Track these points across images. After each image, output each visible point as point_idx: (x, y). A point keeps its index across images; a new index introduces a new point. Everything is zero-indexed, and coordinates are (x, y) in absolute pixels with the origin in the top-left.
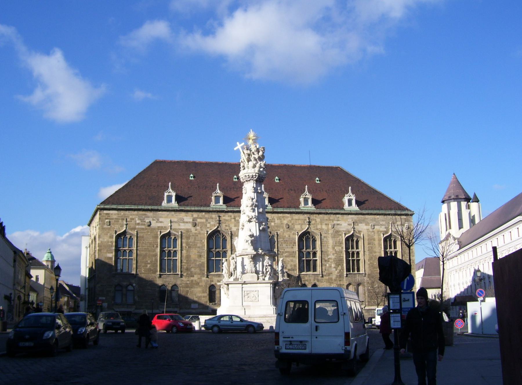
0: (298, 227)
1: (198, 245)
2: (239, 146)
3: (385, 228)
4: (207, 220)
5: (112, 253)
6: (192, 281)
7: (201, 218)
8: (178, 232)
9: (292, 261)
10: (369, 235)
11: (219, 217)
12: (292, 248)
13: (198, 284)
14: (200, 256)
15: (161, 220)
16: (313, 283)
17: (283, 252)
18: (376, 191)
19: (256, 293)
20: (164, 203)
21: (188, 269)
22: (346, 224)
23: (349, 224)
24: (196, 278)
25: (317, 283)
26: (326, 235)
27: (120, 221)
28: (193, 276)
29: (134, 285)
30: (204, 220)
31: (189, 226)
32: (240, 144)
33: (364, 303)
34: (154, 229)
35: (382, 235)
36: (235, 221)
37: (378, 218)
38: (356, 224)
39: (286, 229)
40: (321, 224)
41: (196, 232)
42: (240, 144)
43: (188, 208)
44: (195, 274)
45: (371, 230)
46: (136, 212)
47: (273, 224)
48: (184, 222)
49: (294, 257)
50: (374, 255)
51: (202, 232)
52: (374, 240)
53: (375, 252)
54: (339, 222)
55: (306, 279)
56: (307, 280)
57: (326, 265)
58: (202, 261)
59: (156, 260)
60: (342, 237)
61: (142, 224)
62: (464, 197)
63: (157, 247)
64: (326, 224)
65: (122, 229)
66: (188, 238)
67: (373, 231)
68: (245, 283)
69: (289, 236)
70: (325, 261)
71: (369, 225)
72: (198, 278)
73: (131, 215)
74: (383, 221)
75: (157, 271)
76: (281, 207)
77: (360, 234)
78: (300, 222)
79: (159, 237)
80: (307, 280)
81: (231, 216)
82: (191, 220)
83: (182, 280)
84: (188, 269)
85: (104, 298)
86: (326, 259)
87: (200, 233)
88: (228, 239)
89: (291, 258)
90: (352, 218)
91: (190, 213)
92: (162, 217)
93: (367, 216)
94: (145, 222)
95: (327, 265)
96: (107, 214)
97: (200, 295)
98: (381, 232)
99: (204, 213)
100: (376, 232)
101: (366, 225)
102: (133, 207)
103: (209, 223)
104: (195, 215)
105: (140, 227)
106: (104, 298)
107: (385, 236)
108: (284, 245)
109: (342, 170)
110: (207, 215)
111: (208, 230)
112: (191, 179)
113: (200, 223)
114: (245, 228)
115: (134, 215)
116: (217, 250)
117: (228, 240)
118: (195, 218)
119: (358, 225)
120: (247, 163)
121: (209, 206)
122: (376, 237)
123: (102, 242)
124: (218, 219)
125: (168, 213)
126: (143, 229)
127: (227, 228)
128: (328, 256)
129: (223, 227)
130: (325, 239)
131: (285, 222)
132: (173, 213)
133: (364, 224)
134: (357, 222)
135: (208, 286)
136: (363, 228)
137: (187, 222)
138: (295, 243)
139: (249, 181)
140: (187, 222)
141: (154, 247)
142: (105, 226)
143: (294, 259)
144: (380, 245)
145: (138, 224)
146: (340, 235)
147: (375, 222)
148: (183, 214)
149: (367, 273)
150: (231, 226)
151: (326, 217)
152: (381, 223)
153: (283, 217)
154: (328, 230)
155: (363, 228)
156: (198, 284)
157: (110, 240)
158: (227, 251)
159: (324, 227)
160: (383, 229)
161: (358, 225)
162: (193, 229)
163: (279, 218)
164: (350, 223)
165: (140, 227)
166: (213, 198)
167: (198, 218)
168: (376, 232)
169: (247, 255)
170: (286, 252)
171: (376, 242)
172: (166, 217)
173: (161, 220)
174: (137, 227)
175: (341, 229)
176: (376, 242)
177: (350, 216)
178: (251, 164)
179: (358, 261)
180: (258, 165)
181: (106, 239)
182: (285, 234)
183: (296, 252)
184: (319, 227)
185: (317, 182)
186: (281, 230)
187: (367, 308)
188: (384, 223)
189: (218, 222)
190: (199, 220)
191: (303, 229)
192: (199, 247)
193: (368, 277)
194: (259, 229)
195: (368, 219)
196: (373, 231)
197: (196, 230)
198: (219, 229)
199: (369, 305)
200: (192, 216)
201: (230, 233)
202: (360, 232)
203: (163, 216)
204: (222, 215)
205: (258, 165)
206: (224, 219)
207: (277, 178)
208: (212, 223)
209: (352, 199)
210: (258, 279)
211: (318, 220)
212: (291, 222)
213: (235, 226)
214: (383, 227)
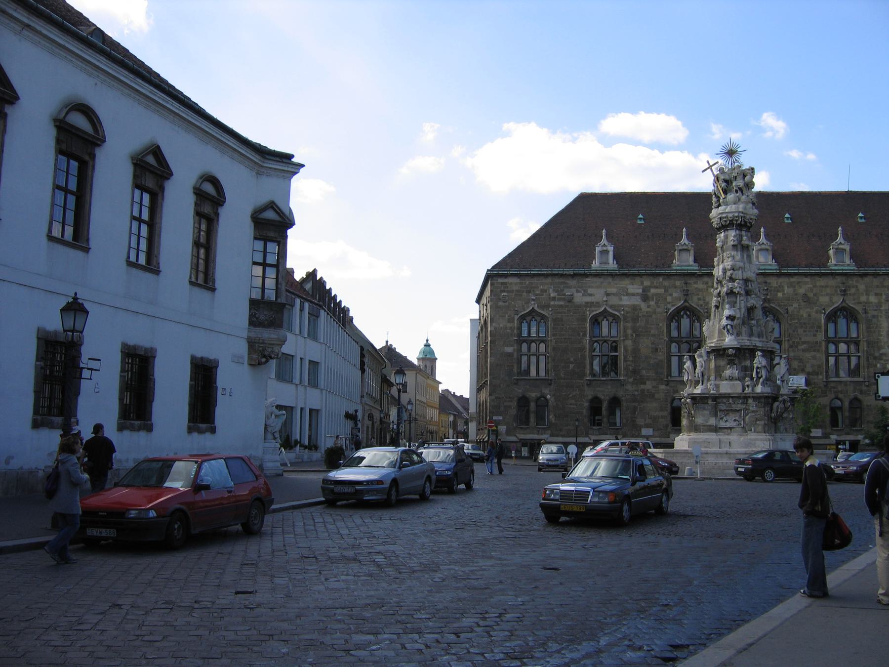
0: (824, 300)
1: (652, 332)
4: (666, 291)
5: (512, 346)
6: (643, 391)
7: (656, 287)
8: (619, 311)
9: (814, 358)
12: (815, 335)
13: (652, 396)
14: (656, 350)
15: (590, 291)
16: (852, 396)
17: (798, 343)
20: (596, 264)
21: (635, 372)
24: (648, 386)
25: (860, 396)
26: (875, 313)
27: (525, 294)
28: (645, 384)
29: (548, 397)
30: (661, 291)
31: (637, 301)
34: (579, 306)
39: (803, 304)
40: (868, 295)
41: (649, 310)
43: (634, 271)
44: (648, 379)
46: (549, 280)
47: (780, 295)
48: (628, 294)
49: (818, 351)
51: (659, 310)
55: (840, 389)
56: (841, 392)
57: (876, 366)
58: (659, 358)
59: (584, 357)
61: (559, 300)
63: (585, 335)
64: (876, 294)
65: (528, 307)
66: (635, 320)
69: (809, 315)
70: (875, 358)
72: (653, 387)
75: (585, 375)
76: (794, 266)
78: (828, 291)
80: (841, 392)
81: (707, 283)
82: (640, 291)
83: (627, 390)
84: (635, 372)
85: (501, 418)
86: (877, 354)
87: (655, 312)
89: (813, 353)
91: (638, 279)
92: (592, 287)
94: (564, 295)
95: (878, 365)
96: (502, 284)
97: (657, 413)
99: (661, 279)
102: (545, 271)
103: (671, 295)
104: (647, 283)
106: (501, 418)
108: (800, 331)
110: (666, 283)
111: (669, 306)
112: (639, 222)
113: (657, 294)
118: (646, 287)
121: (669, 267)
123: (495, 328)
125: (601, 280)
126: (561, 306)
127: (701, 302)
128: (879, 348)
129: (694, 302)
130: (874, 320)
131: (802, 291)
132: (610, 279)
135: (669, 399)
137: (633, 295)
138: (820, 327)
140: (633, 295)
141: (579, 335)
142: (501, 303)
143: (818, 355)
145: (554, 299)
148: (626, 283)
151: (876, 281)
153: (799, 283)
154: (879, 305)
156: (652, 396)
157: (509, 325)
159: (873, 299)
162: (643, 306)
163: (791, 285)
167: (651, 287)
170: (804, 343)
172: (598, 287)
173: (590, 291)
174: (552, 303)
181: (503, 323)
182: (802, 312)
183: (821, 343)
184: (863, 298)
185: (860, 221)
186: (796, 305)
190: (653, 291)
191: (833, 304)
192: (654, 335)
197: (649, 307)
200: (642, 283)
204: (691, 281)
207: (787, 215)
208: (675, 295)
210: (744, 390)
211: (862, 287)
212: (812, 291)
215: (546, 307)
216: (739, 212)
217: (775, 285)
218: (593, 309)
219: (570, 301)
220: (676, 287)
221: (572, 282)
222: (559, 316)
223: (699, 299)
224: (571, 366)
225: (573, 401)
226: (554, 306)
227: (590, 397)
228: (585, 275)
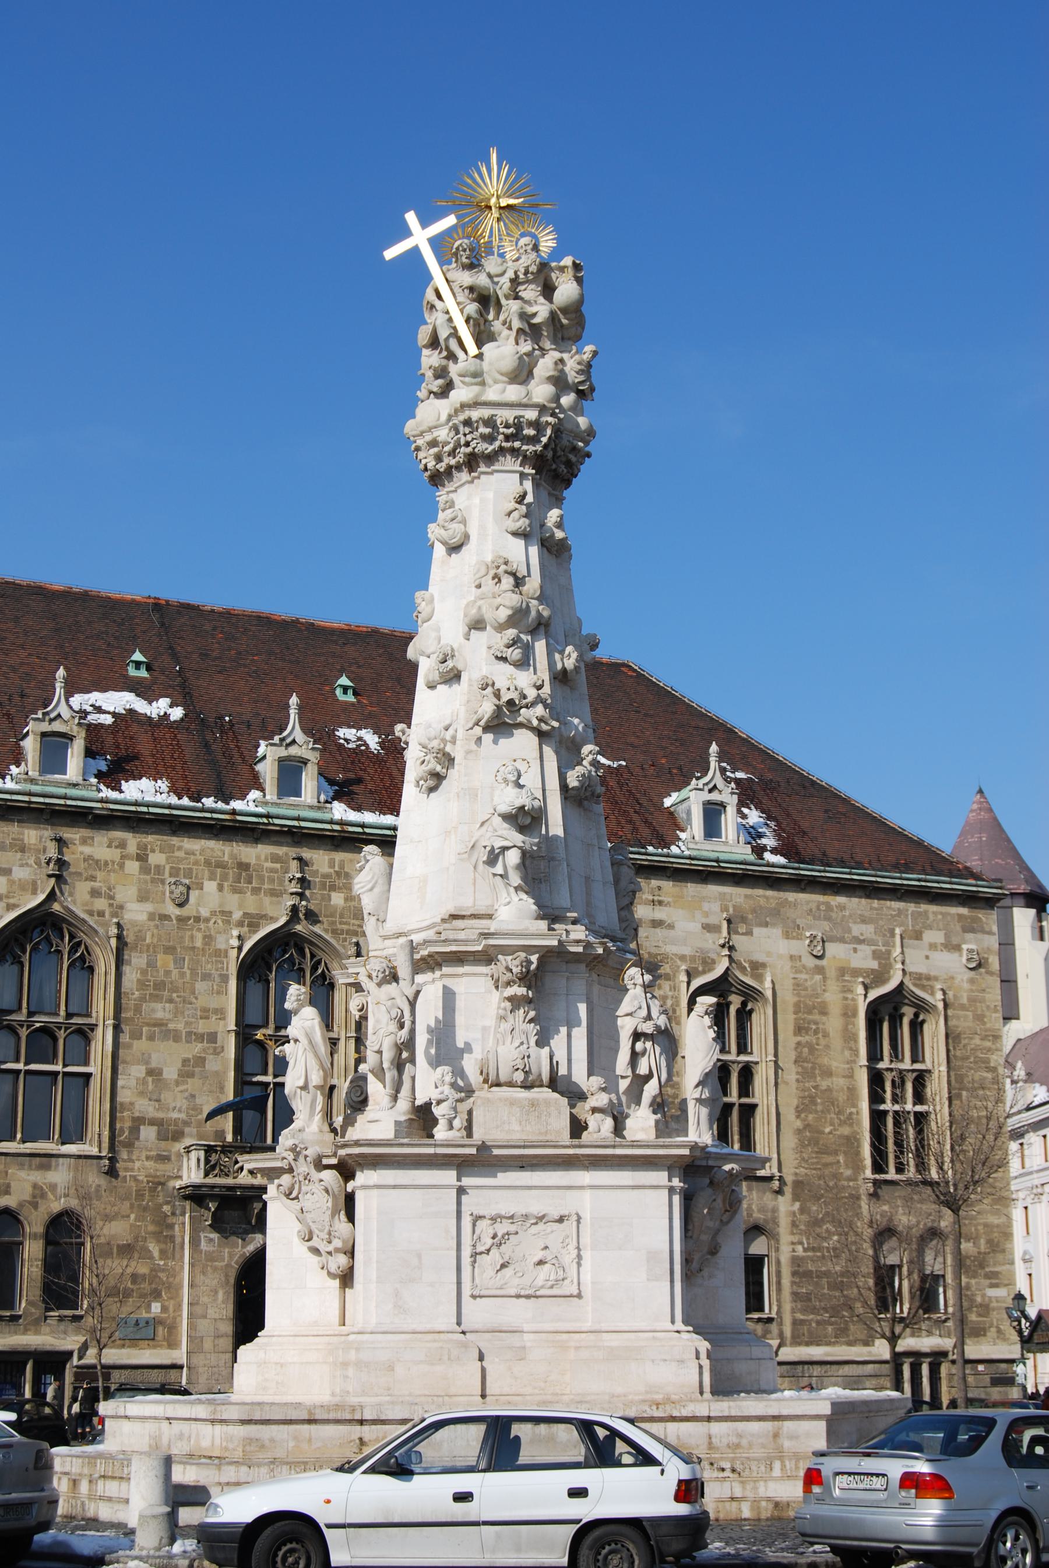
2: (420, 236)
3: (876, 955)
10: (798, 986)
11: (60, 842)
18: (813, 783)
19: (555, 1234)
22: (695, 927)
23: (708, 928)
32: (425, 223)
33: (774, 1327)
35: (860, 990)
36: (145, 869)
37: (842, 908)
38: (742, 928)
42: (425, 223)
45: (811, 962)
50: (824, 1084)
52: (824, 1012)
53: (828, 1073)
54: (659, 914)
60: (674, 988)
62: (1023, 888)
67: (820, 970)
68: (481, 1161)
71: (800, 937)
74: (864, 921)
77: (760, 978)
81: (122, 845)
88: (104, 962)
90: (722, 896)
93: (792, 896)
98: (856, 972)
100: (832, 973)
101: (787, 936)
107: (873, 995)
109: (641, 679)
114: (454, 777)
116: (40, 1020)
117: (100, 968)
119: (749, 933)
120: (472, 349)
122: (832, 997)
124: (52, 852)
127: (101, 904)
129: (77, 900)
133: (776, 932)
134: (743, 919)
136: (774, 951)
139: (490, 458)
144: (850, 1037)
146: (667, 977)
147: (826, 925)
149: (789, 1179)
150: (119, 897)
152: (857, 929)
155: (774, 951)
158: (93, 1027)
160: (864, 959)
161: (749, 933)
164: (713, 920)
166: (30, 745)
168: (832, 973)
169: (487, 957)
171: (833, 1024)
175: (671, 949)
176: (833, 1024)
177: (713, 889)
178: (504, 351)
179: (748, 1111)
180: (545, 366)
187: (789, 1353)
188: (867, 930)
189: (52, 869)
193: (796, 1197)
194: (564, 787)
195: (795, 904)
196: (820, 970)
198: (56, 907)
199: (797, 1340)
201: (114, 931)
202: (757, 967)
205: (545, 366)
206: (88, 859)
207: (344, 681)
208: (20, 873)
209: (723, 806)
210: (577, 1128)
213: (143, 898)
214: (866, 950)
216: (542, 409)
217: (325, 869)
220: (23, 849)
223: (95, 893)
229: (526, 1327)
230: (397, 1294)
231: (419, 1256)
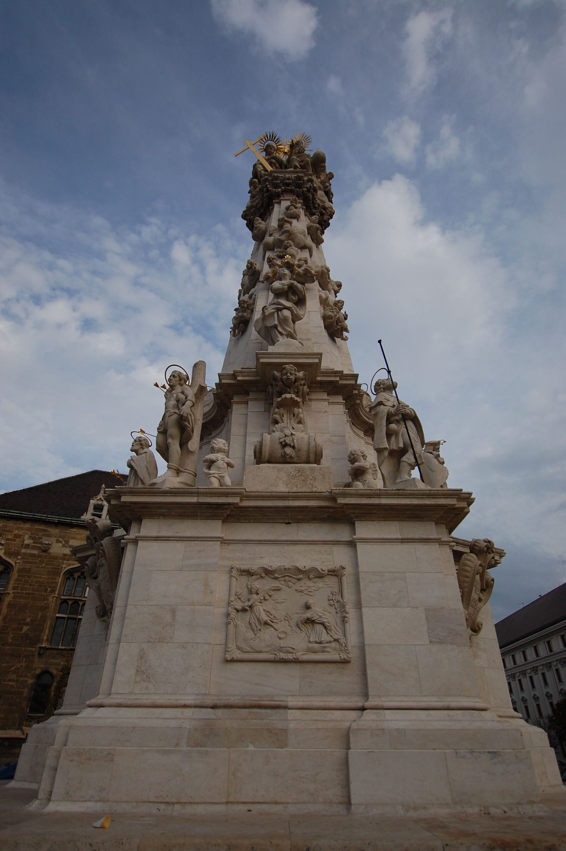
20: (87, 517)
34: (56, 558)
46: (28, 525)
61: (34, 548)
63: (53, 591)
73: (18, 529)
75: (39, 641)
79: (62, 573)
92: (76, 539)
94: (41, 543)
102: (25, 514)
105: (29, 551)
115: (22, 529)
126: (33, 555)
141: (46, 590)
145: (27, 546)
165: (29, 551)
174: (23, 551)
203: (79, 536)
215: (15, 554)
218: (71, 562)
219: (45, 551)
221: (54, 531)
222: (28, 566)
224: (25, 628)
225: (14, 676)
226: (25, 554)
227: (38, 672)
228: (71, 525)
229: (291, 702)
230: (142, 656)
231: (173, 612)
